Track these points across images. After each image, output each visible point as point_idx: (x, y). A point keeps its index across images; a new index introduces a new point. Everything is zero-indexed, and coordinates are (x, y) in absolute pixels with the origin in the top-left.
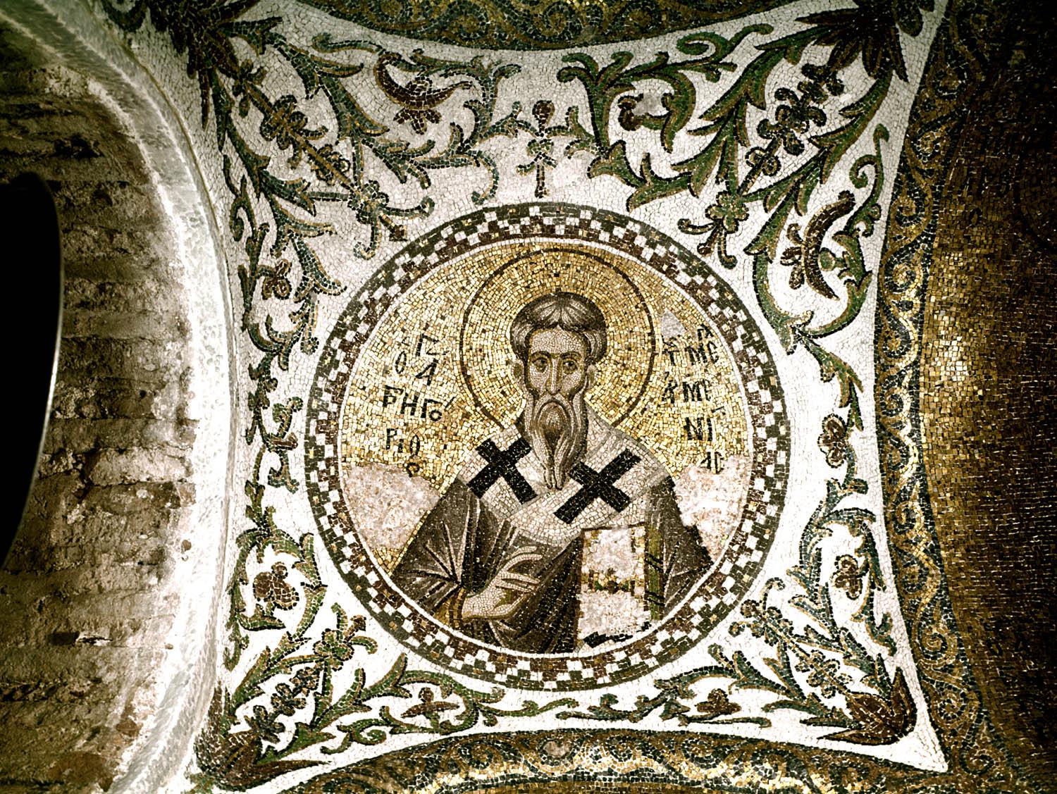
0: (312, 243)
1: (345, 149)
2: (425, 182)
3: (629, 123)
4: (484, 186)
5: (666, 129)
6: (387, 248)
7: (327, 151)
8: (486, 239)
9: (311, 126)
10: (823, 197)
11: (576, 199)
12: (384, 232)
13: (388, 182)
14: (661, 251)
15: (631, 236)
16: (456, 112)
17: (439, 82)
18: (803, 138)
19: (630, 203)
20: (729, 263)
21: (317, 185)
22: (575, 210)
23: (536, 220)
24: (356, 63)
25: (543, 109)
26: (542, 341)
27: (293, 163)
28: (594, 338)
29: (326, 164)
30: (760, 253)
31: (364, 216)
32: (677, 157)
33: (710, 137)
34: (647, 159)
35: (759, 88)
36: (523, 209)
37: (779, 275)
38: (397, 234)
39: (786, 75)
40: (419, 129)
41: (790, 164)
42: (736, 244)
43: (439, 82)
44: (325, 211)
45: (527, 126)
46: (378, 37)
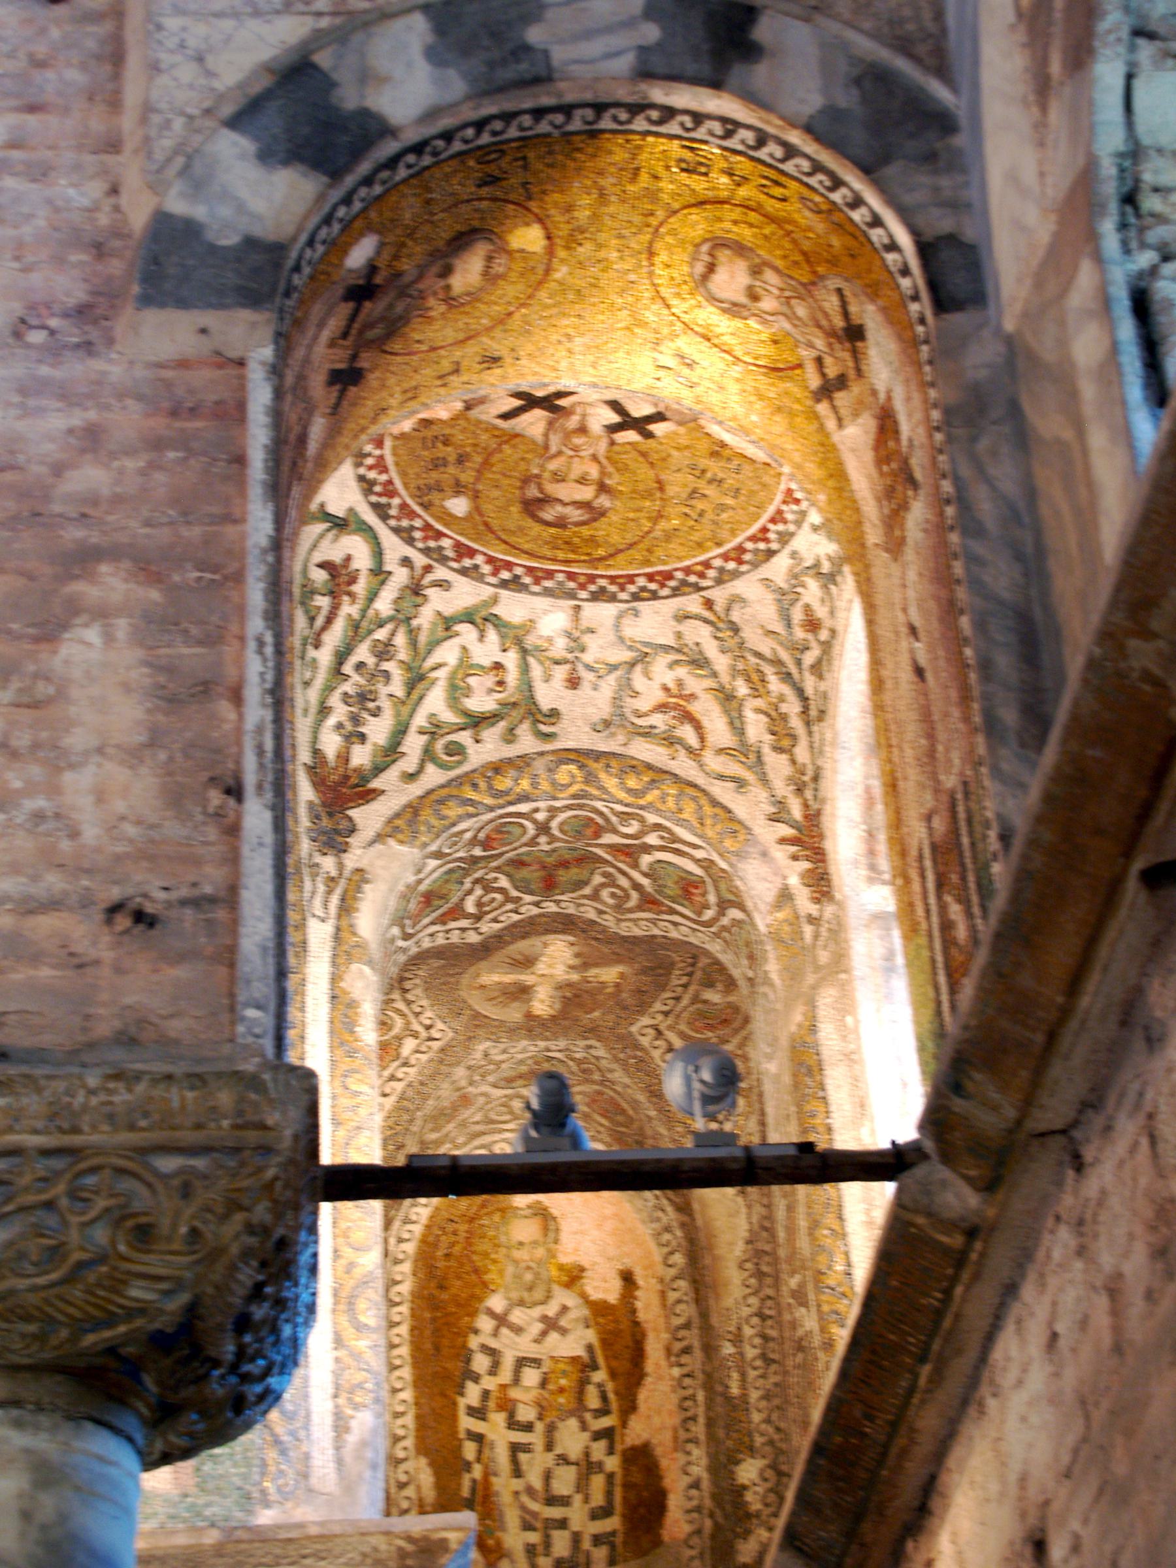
0: (779, 627)
1: (742, 689)
2: (679, 635)
3: (498, 666)
4: (627, 621)
5: (466, 666)
6: (719, 595)
7: (756, 693)
8: (631, 579)
9: (764, 719)
10: (334, 636)
11: (543, 602)
12: (719, 607)
13: (711, 649)
14: (467, 562)
15: (495, 573)
16: (649, 689)
17: (659, 721)
18: (356, 678)
19: (495, 600)
20: (406, 562)
21: (769, 670)
22: (548, 592)
23: (582, 587)
24: (722, 758)
25: (573, 683)
26: (586, 493)
27: (782, 698)
28: (533, 492)
29: (758, 685)
30: (380, 573)
31: (735, 629)
32: (456, 641)
33: (430, 662)
34: (482, 638)
35: (398, 714)
36: (595, 597)
37: (362, 560)
38: (709, 604)
39: (378, 730)
40: (680, 683)
41: (362, 653)
42: (400, 577)
43: (659, 721)
44: (765, 646)
45: (589, 668)
46: (701, 780)
